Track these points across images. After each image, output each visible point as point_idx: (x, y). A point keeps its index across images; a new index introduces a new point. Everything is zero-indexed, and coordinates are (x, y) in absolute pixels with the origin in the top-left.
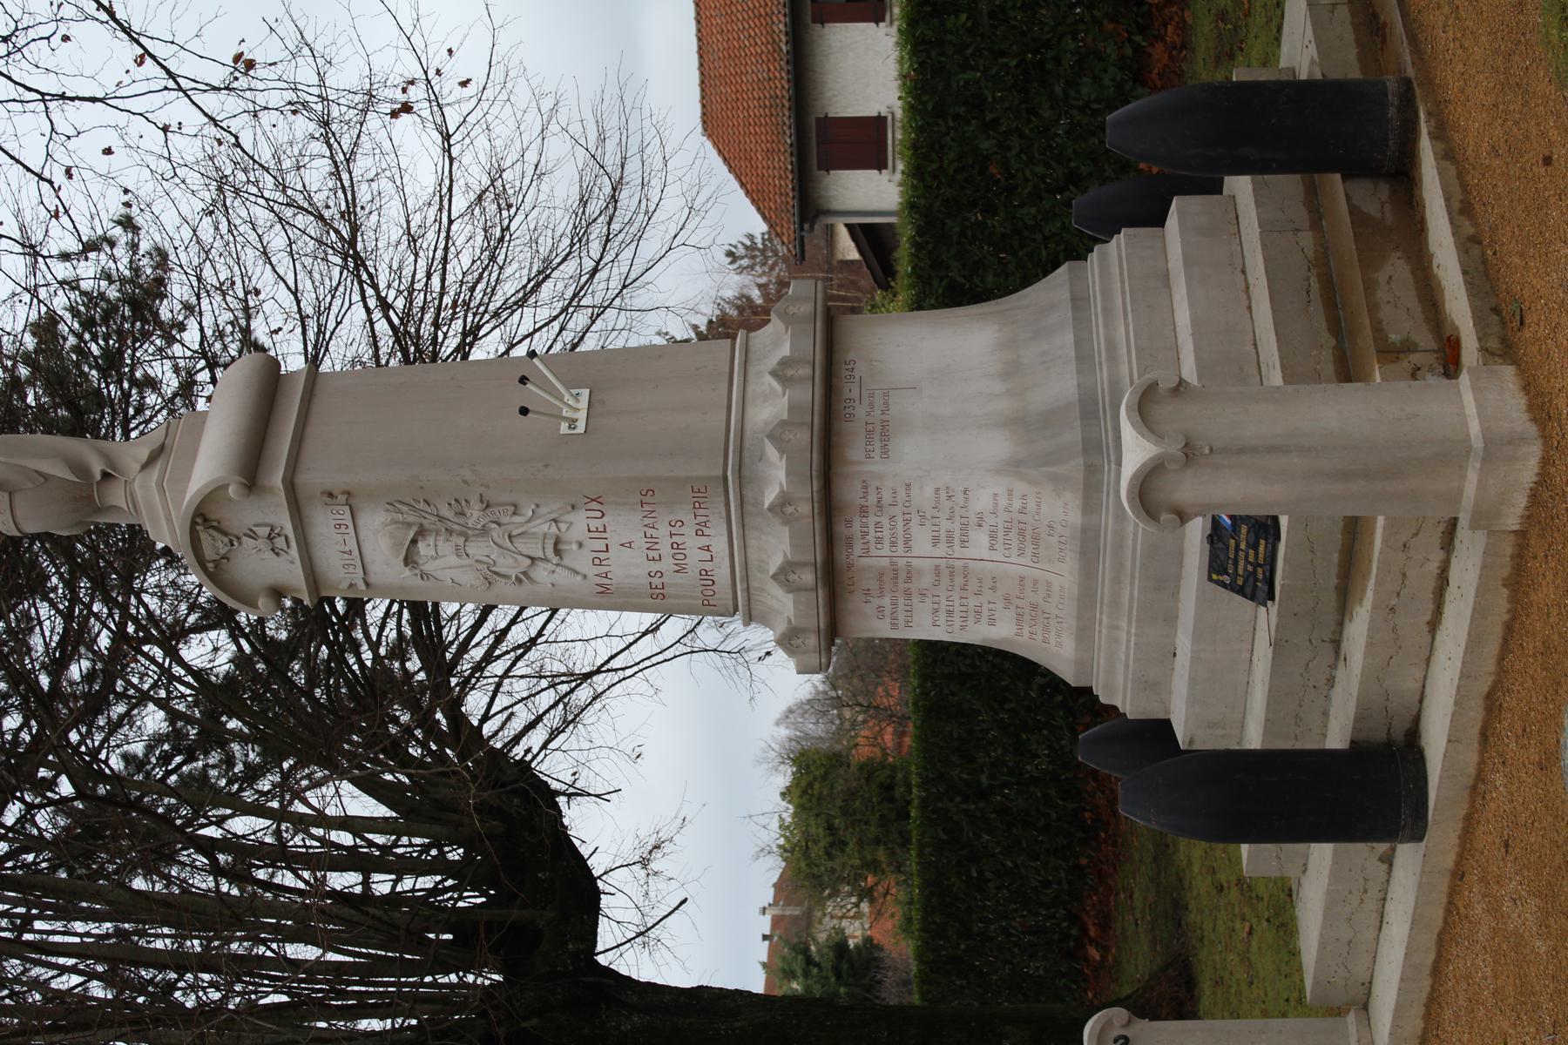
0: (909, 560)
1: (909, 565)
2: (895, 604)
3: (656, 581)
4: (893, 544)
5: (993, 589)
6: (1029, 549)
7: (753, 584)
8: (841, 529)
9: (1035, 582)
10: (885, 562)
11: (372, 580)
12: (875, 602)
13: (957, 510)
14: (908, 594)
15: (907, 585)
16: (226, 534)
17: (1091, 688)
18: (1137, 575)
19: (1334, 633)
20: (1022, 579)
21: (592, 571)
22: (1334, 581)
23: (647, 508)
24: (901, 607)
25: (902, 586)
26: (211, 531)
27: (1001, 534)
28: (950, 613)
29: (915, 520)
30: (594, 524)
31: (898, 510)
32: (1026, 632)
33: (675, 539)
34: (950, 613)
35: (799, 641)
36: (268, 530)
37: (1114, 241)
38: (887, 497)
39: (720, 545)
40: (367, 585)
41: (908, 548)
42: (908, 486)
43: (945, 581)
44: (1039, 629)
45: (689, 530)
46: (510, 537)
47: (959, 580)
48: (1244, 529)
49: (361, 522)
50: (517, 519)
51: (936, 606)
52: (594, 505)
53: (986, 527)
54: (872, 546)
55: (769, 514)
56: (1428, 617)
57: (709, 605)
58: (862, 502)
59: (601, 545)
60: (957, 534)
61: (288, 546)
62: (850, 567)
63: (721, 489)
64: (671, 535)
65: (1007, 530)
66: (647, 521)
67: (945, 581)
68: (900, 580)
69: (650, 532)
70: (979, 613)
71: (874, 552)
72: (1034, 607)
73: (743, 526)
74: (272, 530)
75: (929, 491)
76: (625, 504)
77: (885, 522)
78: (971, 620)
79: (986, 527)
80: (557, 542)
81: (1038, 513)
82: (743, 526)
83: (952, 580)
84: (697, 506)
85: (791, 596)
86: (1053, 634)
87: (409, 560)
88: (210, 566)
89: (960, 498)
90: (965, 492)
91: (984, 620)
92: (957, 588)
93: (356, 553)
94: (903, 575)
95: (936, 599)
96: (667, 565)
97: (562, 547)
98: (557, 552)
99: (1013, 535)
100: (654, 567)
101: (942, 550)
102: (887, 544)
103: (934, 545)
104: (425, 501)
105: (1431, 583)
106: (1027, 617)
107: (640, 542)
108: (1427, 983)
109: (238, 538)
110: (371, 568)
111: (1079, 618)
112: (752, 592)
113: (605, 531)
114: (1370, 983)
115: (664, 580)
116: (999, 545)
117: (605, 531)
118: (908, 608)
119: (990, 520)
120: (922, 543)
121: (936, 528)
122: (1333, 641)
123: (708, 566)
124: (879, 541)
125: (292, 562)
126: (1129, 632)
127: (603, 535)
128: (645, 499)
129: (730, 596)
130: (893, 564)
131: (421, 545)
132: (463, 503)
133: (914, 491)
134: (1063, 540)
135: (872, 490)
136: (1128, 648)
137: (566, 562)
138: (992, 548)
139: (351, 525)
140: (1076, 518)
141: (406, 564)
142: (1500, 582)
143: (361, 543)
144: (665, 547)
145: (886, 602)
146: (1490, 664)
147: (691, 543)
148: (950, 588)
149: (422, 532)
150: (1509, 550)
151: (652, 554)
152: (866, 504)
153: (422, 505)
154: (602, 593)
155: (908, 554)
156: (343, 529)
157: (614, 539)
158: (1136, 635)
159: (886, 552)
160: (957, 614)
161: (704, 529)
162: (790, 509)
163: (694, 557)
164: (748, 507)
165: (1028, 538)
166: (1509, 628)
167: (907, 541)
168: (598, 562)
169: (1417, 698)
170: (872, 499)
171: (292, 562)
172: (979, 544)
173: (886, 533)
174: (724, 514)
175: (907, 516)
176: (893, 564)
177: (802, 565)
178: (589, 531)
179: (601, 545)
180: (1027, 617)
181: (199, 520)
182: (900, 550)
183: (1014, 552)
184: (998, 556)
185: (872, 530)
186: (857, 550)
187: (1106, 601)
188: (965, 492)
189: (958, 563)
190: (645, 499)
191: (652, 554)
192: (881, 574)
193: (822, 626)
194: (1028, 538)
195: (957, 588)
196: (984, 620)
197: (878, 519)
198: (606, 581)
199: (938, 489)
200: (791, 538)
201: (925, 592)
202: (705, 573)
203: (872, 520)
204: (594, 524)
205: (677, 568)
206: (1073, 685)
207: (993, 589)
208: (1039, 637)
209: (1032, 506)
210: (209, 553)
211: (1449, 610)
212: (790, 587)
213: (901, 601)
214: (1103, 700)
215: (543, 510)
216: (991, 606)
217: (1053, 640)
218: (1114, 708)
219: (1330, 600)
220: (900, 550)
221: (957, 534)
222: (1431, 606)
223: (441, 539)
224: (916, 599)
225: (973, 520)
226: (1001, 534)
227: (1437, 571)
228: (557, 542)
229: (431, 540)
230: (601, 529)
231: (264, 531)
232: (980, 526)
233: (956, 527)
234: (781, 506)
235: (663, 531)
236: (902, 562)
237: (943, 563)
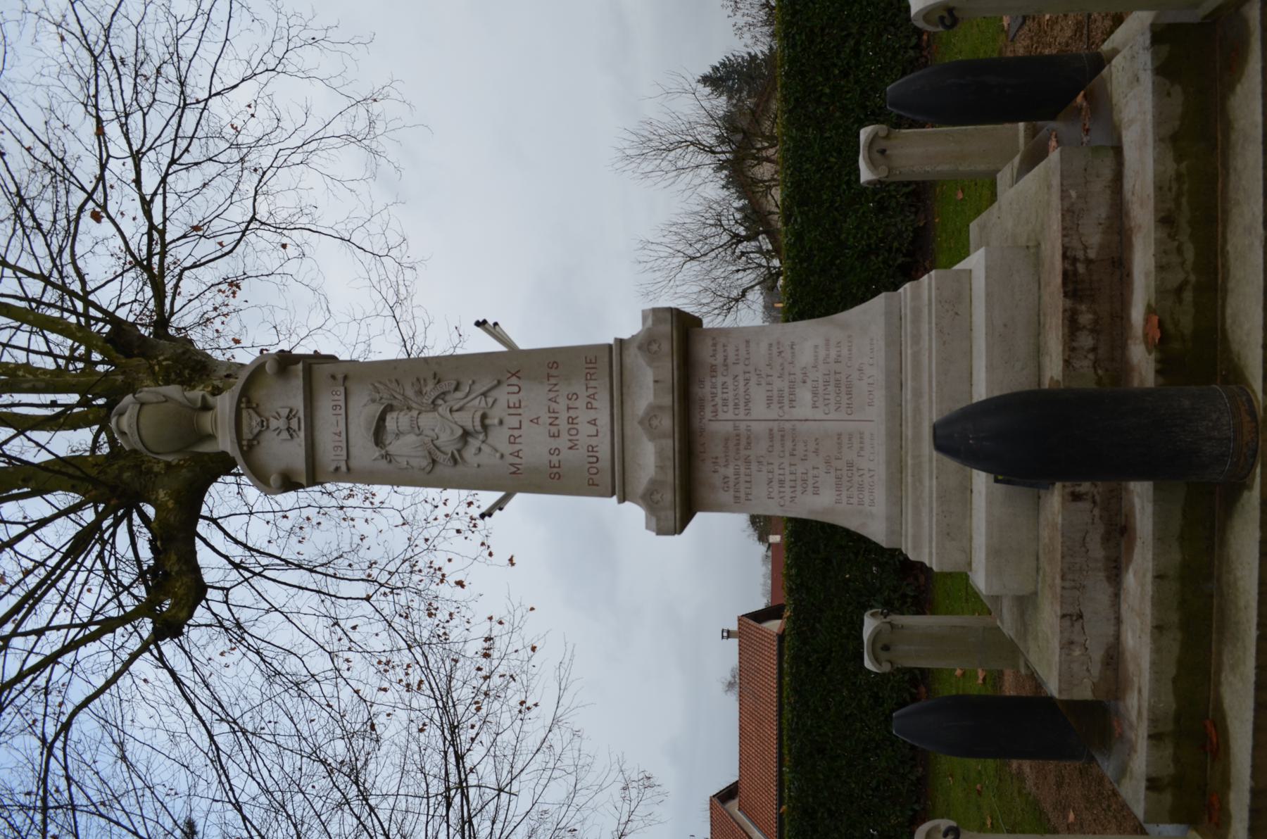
0: (749, 423)
2: (737, 474)
3: (555, 459)
5: (816, 452)
6: (844, 400)
10: (729, 427)
11: (353, 464)
14: (747, 461)
15: (748, 452)
18: (934, 398)
20: (839, 435)
21: (507, 449)
23: (553, 381)
24: (743, 478)
25: (743, 453)
26: (251, 411)
27: (821, 388)
28: (781, 482)
32: (844, 500)
33: (572, 413)
34: (781, 482)
35: (659, 496)
36: (288, 410)
37: (901, 290)
38: (731, 358)
40: (348, 469)
41: (748, 411)
42: (748, 342)
45: (581, 403)
46: (451, 411)
47: (789, 444)
49: (351, 404)
50: (459, 395)
51: (770, 476)
52: (514, 380)
54: (720, 408)
57: (593, 485)
58: (711, 360)
59: (514, 422)
60: (786, 394)
61: (299, 429)
64: (569, 408)
65: (827, 383)
66: (552, 395)
68: (742, 447)
69: (554, 405)
70: (804, 481)
71: (721, 416)
74: (291, 411)
75: (763, 347)
77: (729, 380)
78: (799, 489)
79: (809, 383)
84: (589, 377)
88: (245, 443)
91: (810, 489)
94: (743, 442)
95: (770, 467)
96: (563, 443)
98: (485, 427)
99: (831, 388)
100: (554, 443)
101: (773, 413)
103: (769, 405)
104: (397, 381)
107: (545, 418)
109: (268, 420)
110: (353, 451)
113: (520, 407)
115: (560, 457)
117: (520, 407)
118: (748, 479)
120: (759, 409)
121: (769, 387)
123: (594, 441)
130: (736, 428)
132: (422, 382)
135: (720, 348)
136: (931, 502)
137: (490, 440)
138: (815, 407)
141: (377, 444)
143: (350, 426)
144: (563, 422)
145: (730, 471)
147: (583, 416)
148: (782, 454)
149: (389, 408)
151: (554, 429)
152: (714, 363)
153: (394, 385)
154: (514, 473)
155: (747, 418)
156: (338, 411)
159: (730, 415)
160: (788, 484)
161: (593, 401)
165: (843, 389)
167: (747, 402)
168: (513, 440)
170: (720, 357)
173: (730, 395)
175: (747, 375)
176: (736, 428)
177: (660, 408)
178: (509, 407)
179: (514, 422)
180: (845, 478)
181: (244, 400)
182: (742, 411)
185: (719, 391)
186: (708, 414)
188: (792, 346)
189: (788, 426)
190: (553, 372)
191: (554, 429)
192: (727, 440)
194: (843, 389)
195: (787, 454)
196: (810, 489)
197: (725, 379)
199: (771, 345)
201: (762, 459)
202: (591, 449)
203: (720, 380)
204: (514, 399)
205: (570, 444)
206: (884, 545)
207: (816, 452)
208: (855, 500)
209: (845, 352)
210: (247, 435)
212: (654, 435)
213: (742, 470)
214: (912, 557)
216: (815, 472)
217: (867, 501)
218: (922, 564)
220: (742, 411)
221: (786, 394)
223: (402, 413)
224: (754, 466)
226: (821, 388)
229: (394, 414)
230: (517, 405)
231: (285, 412)
232: (804, 382)
234: (654, 411)
235: (563, 402)
236: (743, 426)
237: (775, 425)
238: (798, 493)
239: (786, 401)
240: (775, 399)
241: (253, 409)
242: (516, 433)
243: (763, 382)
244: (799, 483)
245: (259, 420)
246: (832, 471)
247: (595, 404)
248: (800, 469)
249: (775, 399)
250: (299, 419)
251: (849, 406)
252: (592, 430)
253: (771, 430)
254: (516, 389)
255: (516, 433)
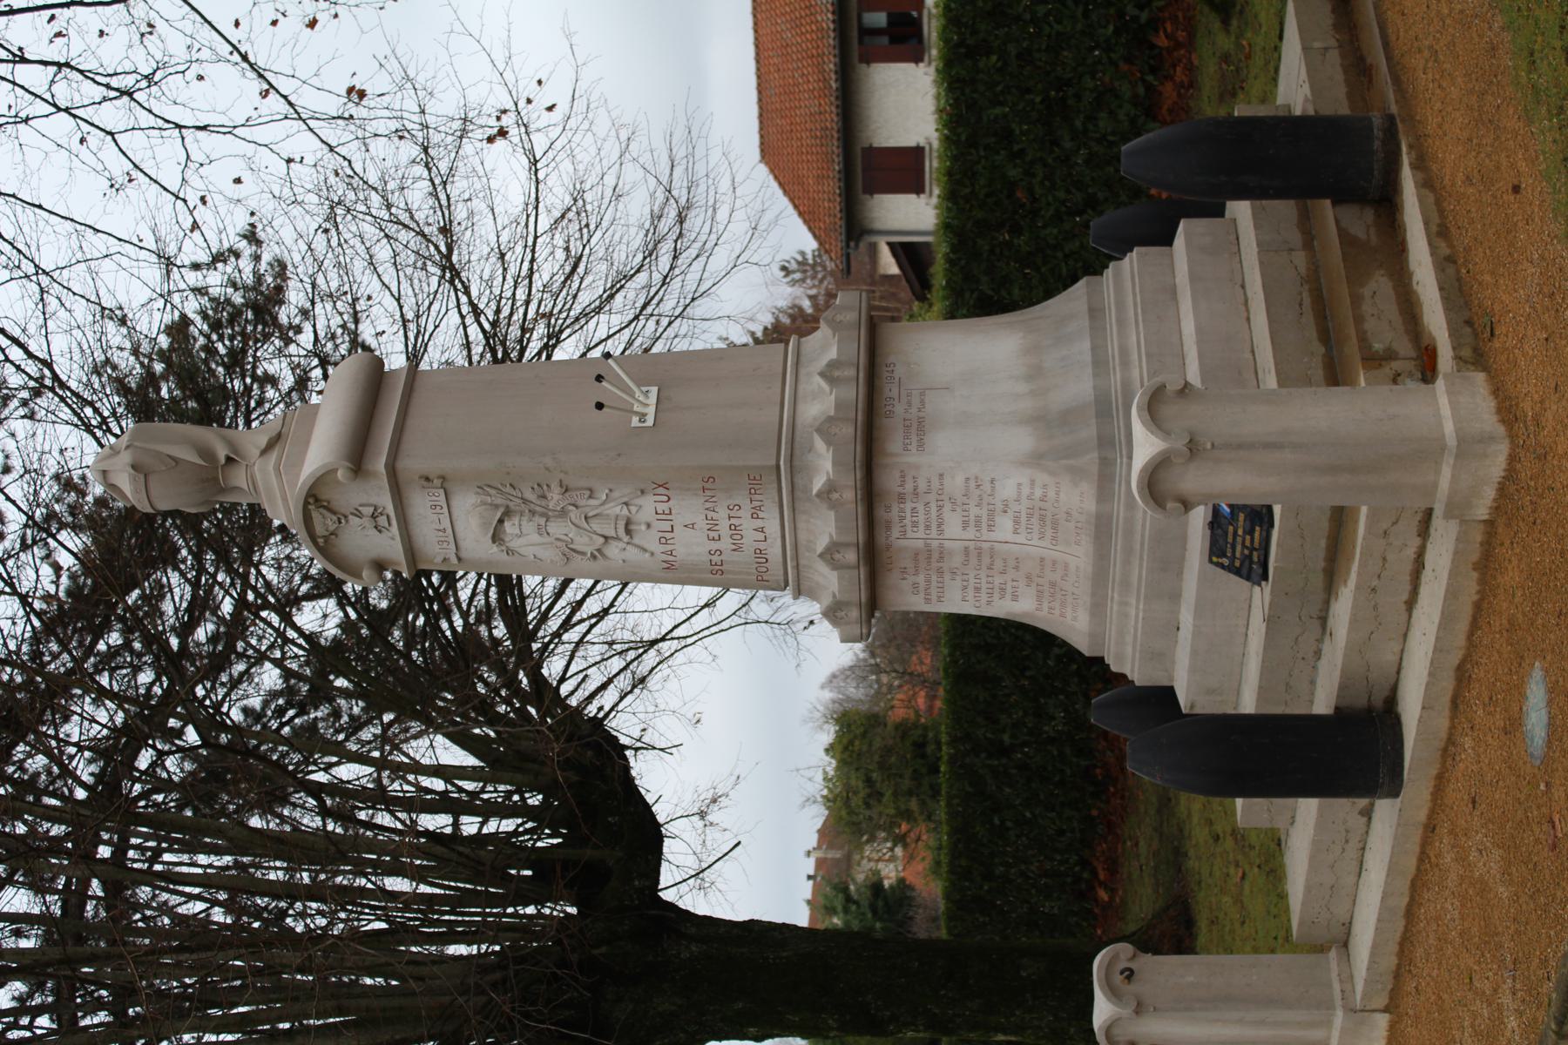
1: (941, 546)
2: (928, 581)
3: (716, 559)
4: (928, 527)
5: (1017, 568)
6: (1049, 533)
7: (802, 562)
8: (880, 513)
9: (1054, 563)
10: (920, 543)
11: (463, 554)
12: (911, 579)
13: (985, 496)
14: (940, 572)
16: (334, 513)
17: (1103, 658)
19: (1321, 610)
20: (1042, 559)
22: (1322, 564)
23: (708, 493)
24: (934, 584)
25: (935, 565)
26: (321, 510)
27: (1023, 519)
28: (977, 589)
29: (948, 506)
30: (661, 507)
31: (932, 497)
32: (1046, 609)
33: (733, 521)
34: (977, 589)
36: (372, 509)
37: (1127, 259)
38: (922, 486)
39: (773, 527)
40: (459, 559)
41: (941, 532)
42: (941, 475)
43: (973, 560)
44: (1057, 605)
45: (745, 513)
46: (586, 518)
47: (986, 560)
48: (1242, 517)
50: (592, 502)
52: (661, 491)
53: (1010, 513)
54: (909, 528)
55: (817, 500)
56: (1405, 597)
58: (900, 490)
59: (666, 526)
60: (984, 519)
62: (889, 547)
63: (774, 477)
65: (1029, 516)
66: (708, 505)
67: (973, 560)
69: (710, 514)
71: (910, 534)
72: (1053, 584)
73: (794, 510)
74: (375, 510)
75: (959, 480)
76: (688, 490)
77: (921, 507)
79: (1010, 513)
80: (628, 523)
81: (1057, 501)
82: (794, 510)
83: (980, 560)
84: (752, 492)
85: (835, 573)
86: (1069, 609)
87: (497, 538)
88: (321, 541)
89: (987, 487)
90: (992, 481)
91: (1008, 596)
92: (984, 567)
93: (449, 531)
94: (935, 556)
95: (965, 577)
96: (726, 544)
97: (632, 527)
98: (628, 532)
99: (1035, 520)
100: (714, 546)
101: (971, 533)
102: (922, 527)
103: (964, 528)
105: (1408, 567)
106: (1046, 594)
107: (701, 523)
108: (1401, 923)
109: (346, 517)
110: (462, 544)
111: (1093, 594)
112: (801, 568)
114: (1350, 923)
116: (1022, 529)
119: (1014, 507)
120: (953, 527)
122: (1320, 618)
123: (762, 546)
124: (915, 524)
125: (393, 539)
126: (1137, 608)
127: (669, 517)
128: (707, 486)
129: (782, 572)
130: (927, 545)
131: (507, 524)
133: (947, 481)
134: (1079, 525)
136: (1136, 622)
137: (636, 540)
138: (1016, 532)
139: (445, 506)
140: (1091, 505)
141: (494, 542)
142: (1470, 566)
143: (455, 523)
144: (724, 525)
145: (921, 579)
146: (1460, 640)
147: (747, 525)
149: (508, 513)
150: (1479, 538)
151: (712, 534)
153: (508, 489)
157: (678, 521)
158: (1144, 611)
160: (984, 590)
162: (835, 496)
163: (750, 537)
164: (798, 494)
165: (1048, 523)
166: (1478, 606)
167: (940, 525)
168: (663, 541)
169: (1395, 669)
170: (909, 487)
171: (393, 539)
172: (1004, 528)
173: (921, 518)
174: (777, 499)
176: (927, 545)
177: (847, 545)
179: (666, 526)
180: (1046, 594)
181: (311, 500)
182: (934, 534)
183: (1036, 536)
184: (1021, 539)
185: (908, 514)
186: (895, 533)
187: (1117, 579)
188: (992, 481)
189: (985, 546)
190: (707, 486)
191: (712, 534)
192: (917, 554)
193: (863, 600)
196: (1008, 596)
198: (671, 558)
199: (968, 479)
200: (836, 521)
202: (759, 552)
203: (908, 506)
204: (661, 507)
206: (1087, 654)
207: (1017, 568)
208: (1057, 612)
209: (1051, 494)
210: (319, 530)
211: (1424, 591)
212: (835, 566)
213: (934, 578)
214: (1114, 668)
215: (616, 494)
218: (1124, 676)
219: (1318, 580)
220: (934, 534)
221: (984, 519)
222: (1408, 587)
223: (525, 519)
224: (947, 577)
225: (999, 506)
226: (1023, 519)
227: (1413, 556)
228: (628, 523)
231: (368, 511)
232: (1005, 512)
233: (984, 513)
234: (830, 488)
235: (722, 514)
236: (935, 544)
238: (996, 595)
239: (984, 525)
240: (972, 523)
241: (324, 507)
242: (668, 535)
243: (959, 509)
244: (997, 590)
245: (335, 518)
246: (1034, 585)
247: (761, 515)
248: (998, 580)
249: (972, 523)
250: (388, 517)
251: (1054, 538)
252: (761, 536)
253: (966, 548)
254: (666, 498)
255: (668, 535)
